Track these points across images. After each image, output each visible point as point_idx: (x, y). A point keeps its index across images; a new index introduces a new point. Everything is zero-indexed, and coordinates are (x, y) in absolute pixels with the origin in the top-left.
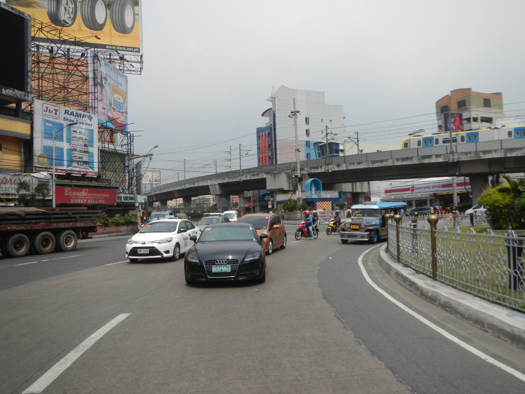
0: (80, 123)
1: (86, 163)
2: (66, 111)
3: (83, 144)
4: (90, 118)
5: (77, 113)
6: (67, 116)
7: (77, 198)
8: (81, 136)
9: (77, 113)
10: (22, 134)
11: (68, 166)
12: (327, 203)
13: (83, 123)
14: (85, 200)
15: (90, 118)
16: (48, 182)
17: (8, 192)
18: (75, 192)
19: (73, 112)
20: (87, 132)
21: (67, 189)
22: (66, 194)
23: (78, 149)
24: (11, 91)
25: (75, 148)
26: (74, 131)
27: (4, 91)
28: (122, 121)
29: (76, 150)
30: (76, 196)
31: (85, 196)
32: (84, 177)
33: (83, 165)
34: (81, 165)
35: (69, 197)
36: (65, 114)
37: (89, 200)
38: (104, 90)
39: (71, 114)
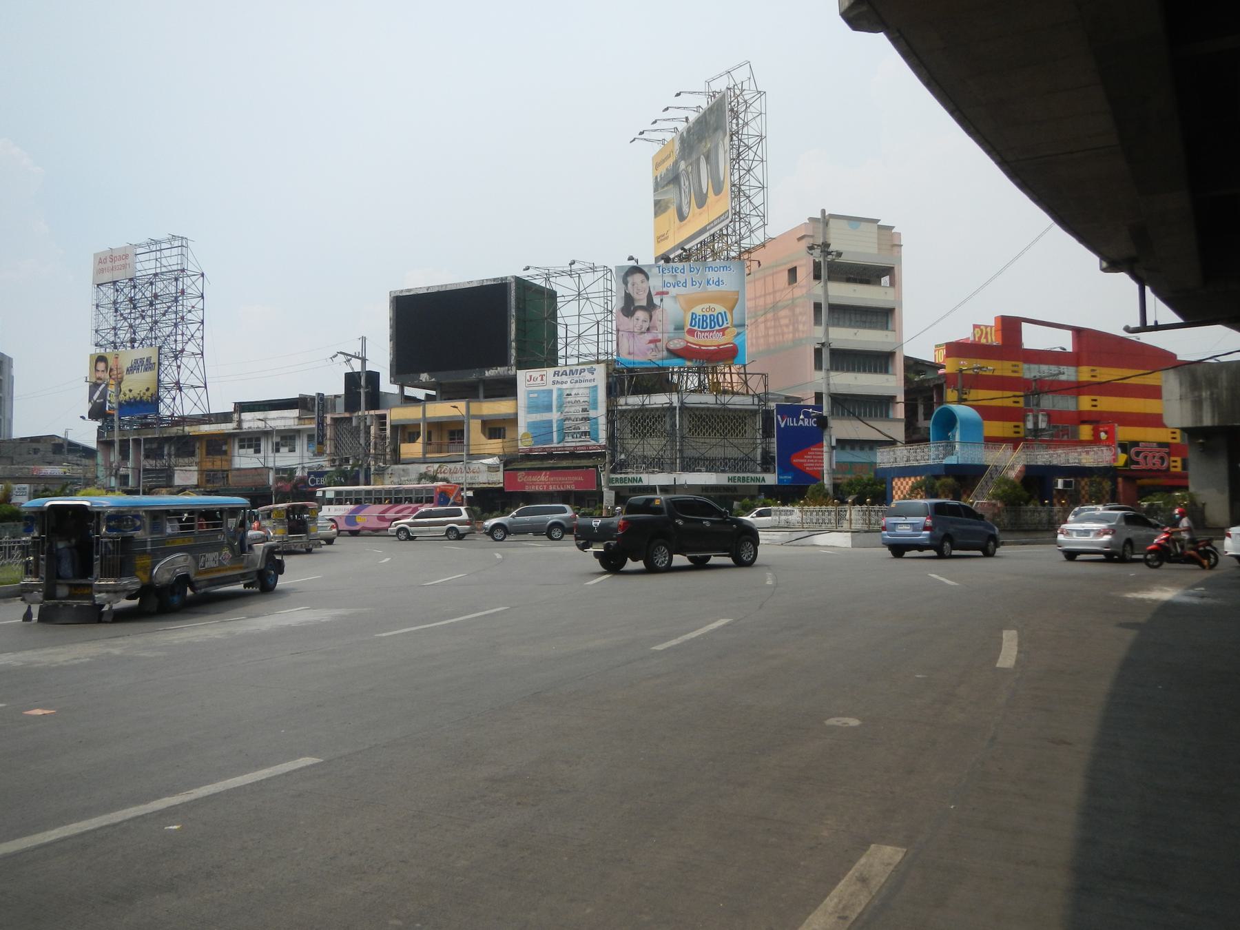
0: (577, 382)
1: (585, 433)
2: (555, 372)
3: (581, 407)
4: (592, 371)
5: (571, 371)
6: (556, 378)
7: (533, 483)
8: (577, 399)
9: (571, 371)
10: (505, 415)
11: (559, 443)
12: (904, 483)
13: (581, 381)
14: (545, 486)
15: (592, 371)
16: (499, 467)
17: (458, 482)
18: (531, 477)
19: (565, 371)
20: (587, 391)
21: (521, 474)
22: (519, 480)
23: (573, 417)
24: (493, 371)
25: (568, 417)
26: (568, 395)
27: (487, 374)
28: (718, 346)
29: (570, 419)
30: (532, 481)
31: (544, 481)
32: (573, 455)
33: (580, 437)
34: (577, 437)
35: (523, 484)
36: (554, 376)
37: (551, 486)
38: (657, 314)
39: (562, 374)
